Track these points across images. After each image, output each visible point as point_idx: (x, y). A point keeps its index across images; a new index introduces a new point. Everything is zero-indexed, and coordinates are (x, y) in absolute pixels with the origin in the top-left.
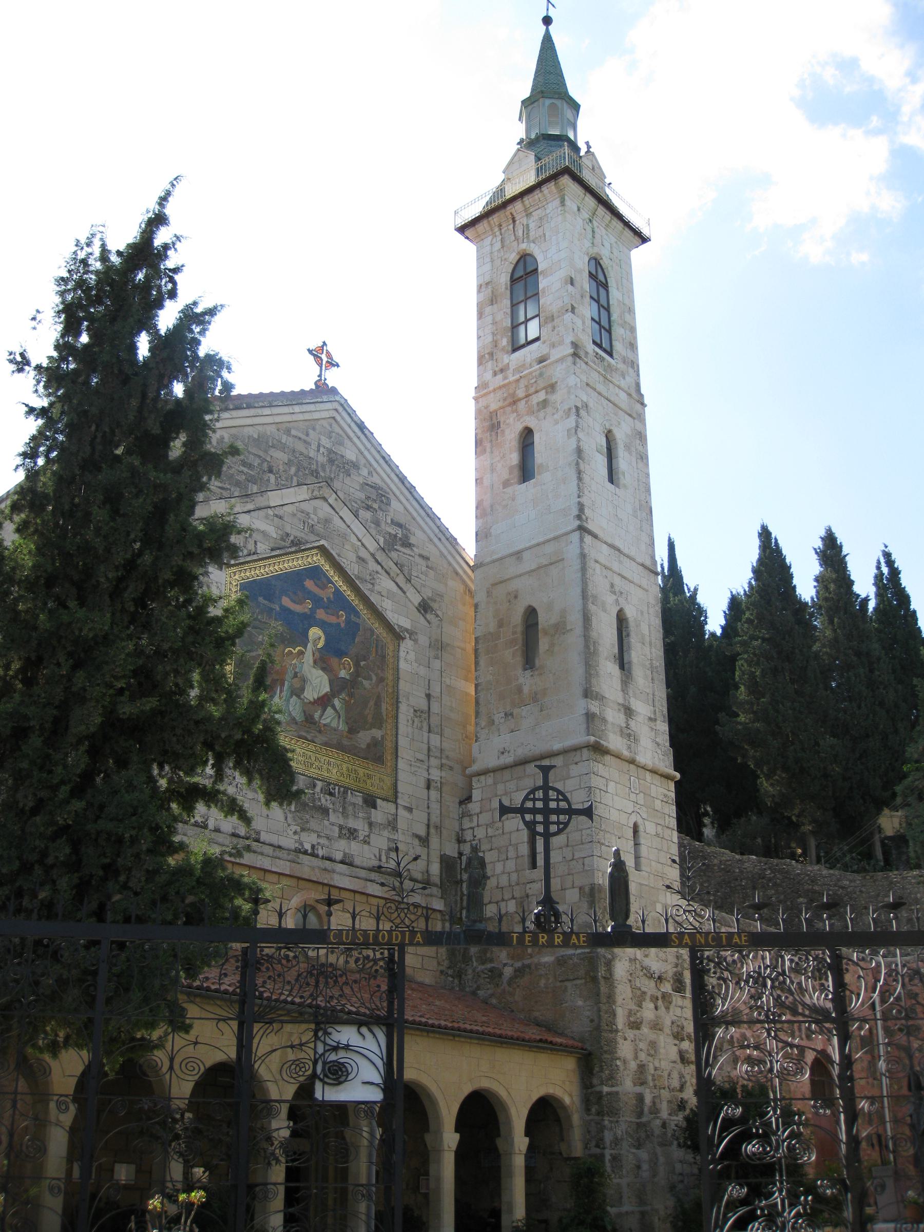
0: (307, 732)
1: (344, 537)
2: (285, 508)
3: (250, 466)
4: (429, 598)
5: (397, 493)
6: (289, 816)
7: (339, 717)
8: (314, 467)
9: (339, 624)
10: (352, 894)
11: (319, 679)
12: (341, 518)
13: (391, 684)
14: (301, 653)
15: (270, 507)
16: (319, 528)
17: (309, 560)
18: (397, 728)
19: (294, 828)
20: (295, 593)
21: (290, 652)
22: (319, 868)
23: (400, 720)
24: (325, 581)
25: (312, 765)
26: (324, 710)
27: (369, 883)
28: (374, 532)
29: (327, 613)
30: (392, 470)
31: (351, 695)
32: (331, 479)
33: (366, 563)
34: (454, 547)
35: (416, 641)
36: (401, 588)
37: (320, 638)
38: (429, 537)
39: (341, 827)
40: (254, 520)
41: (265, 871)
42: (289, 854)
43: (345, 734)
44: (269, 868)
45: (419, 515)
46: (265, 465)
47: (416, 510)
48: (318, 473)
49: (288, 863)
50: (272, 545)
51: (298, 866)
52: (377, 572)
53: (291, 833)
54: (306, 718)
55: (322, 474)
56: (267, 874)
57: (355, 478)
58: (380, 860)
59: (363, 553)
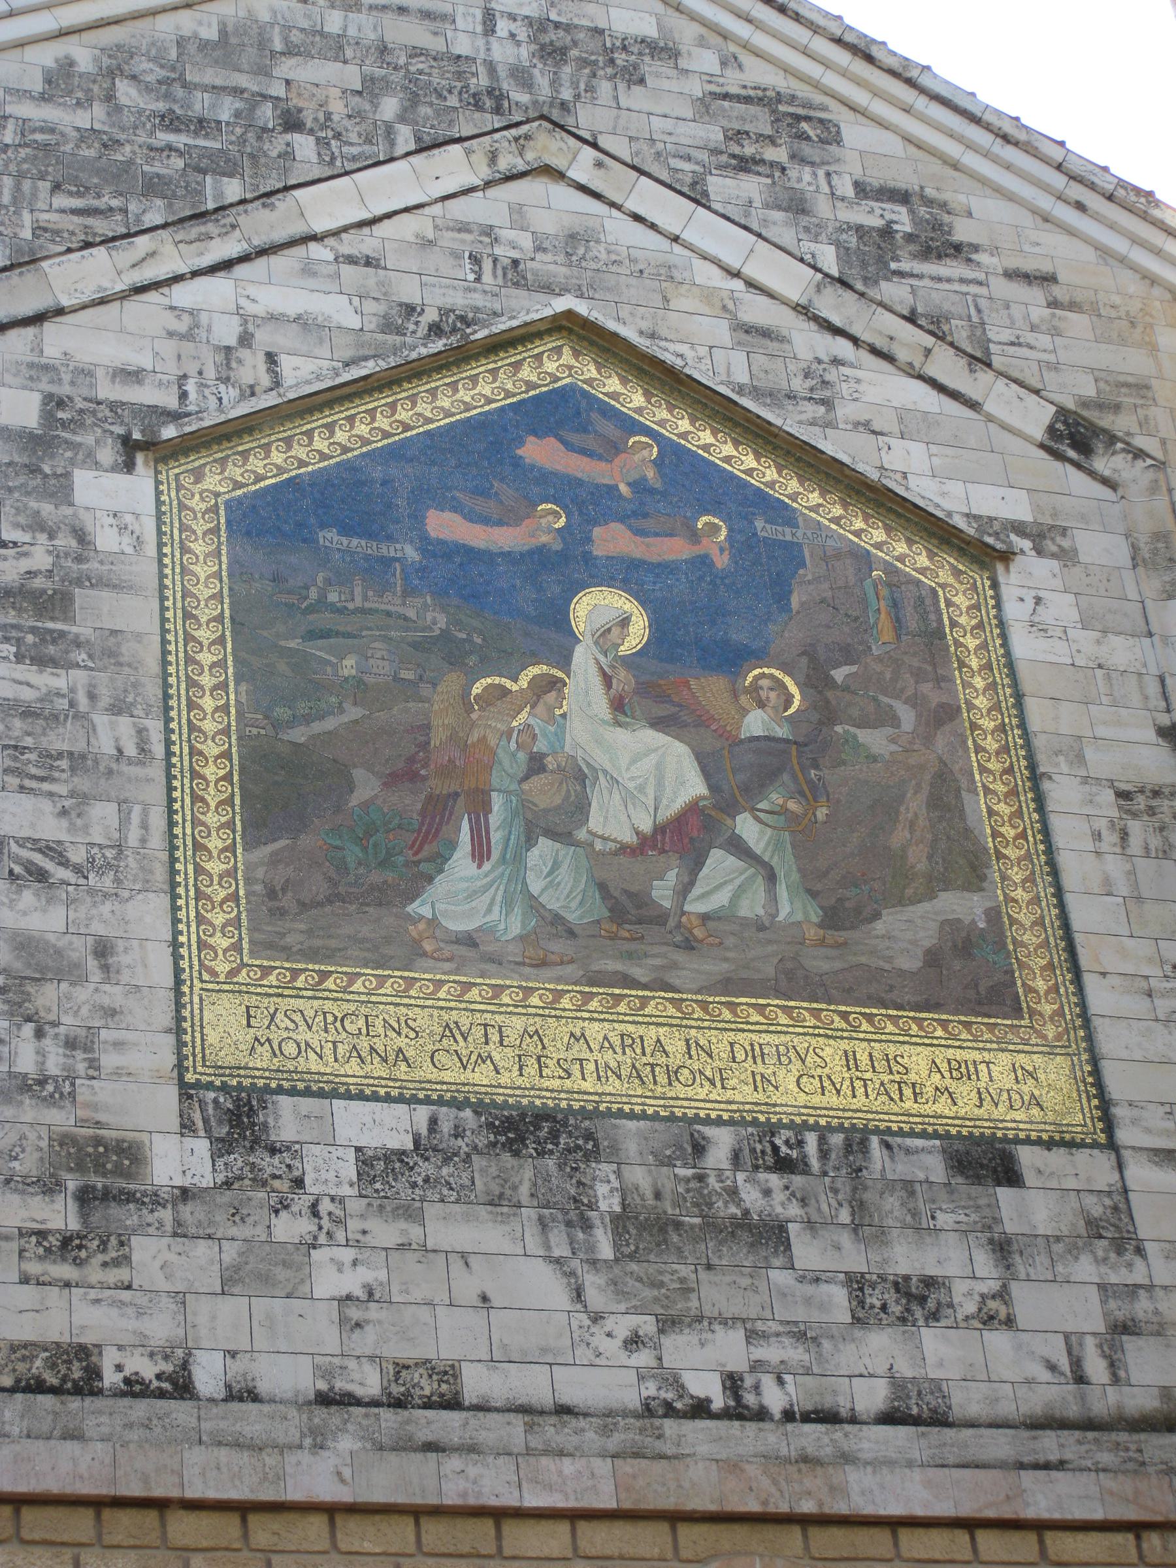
0: (630, 956)
1: (668, 274)
2: (380, 230)
3: (201, 125)
4: (1085, 404)
5: (860, 97)
6: (593, 1283)
7: (771, 877)
8: (484, 81)
9: (704, 561)
10: (963, 1537)
11: (649, 763)
12: (637, 218)
13: (988, 724)
14: (553, 685)
15: (314, 238)
16: (548, 265)
17: (526, 373)
18: (1055, 872)
19: (623, 1326)
20: (482, 492)
21: (504, 692)
22: (771, 1459)
23: (1059, 840)
24: (609, 429)
25: (673, 1075)
26: (699, 864)
27: (1028, 1477)
28: (787, 237)
29: (640, 532)
30: (815, 29)
31: (812, 792)
32: (564, 106)
33: (782, 340)
34: (1144, 216)
35: (1067, 557)
36: (954, 395)
37: (625, 622)
38: (1034, 211)
39: (857, 1284)
40: (252, 290)
41: (499, 1515)
42: (606, 1431)
43: (812, 933)
44: (510, 1499)
45: (970, 146)
46: (267, 114)
47: (951, 135)
48: (498, 100)
49: (603, 1467)
50: (348, 354)
51: (659, 1467)
52: (836, 362)
53: (612, 1347)
54: (618, 914)
55: (523, 98)
56: (510, 1528)
57: (666, 84)
58: (1080, 1379)
59: (757, 311)
